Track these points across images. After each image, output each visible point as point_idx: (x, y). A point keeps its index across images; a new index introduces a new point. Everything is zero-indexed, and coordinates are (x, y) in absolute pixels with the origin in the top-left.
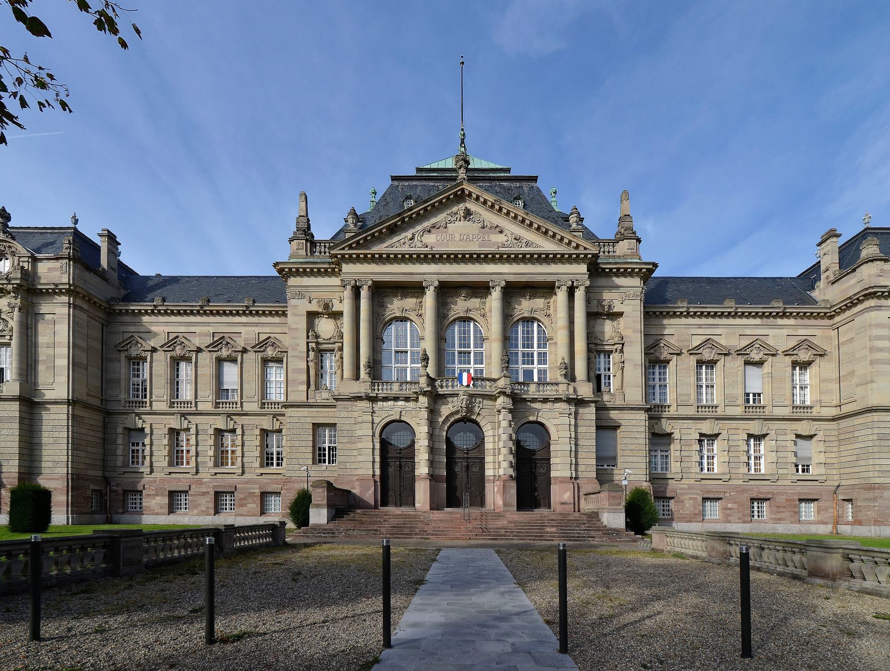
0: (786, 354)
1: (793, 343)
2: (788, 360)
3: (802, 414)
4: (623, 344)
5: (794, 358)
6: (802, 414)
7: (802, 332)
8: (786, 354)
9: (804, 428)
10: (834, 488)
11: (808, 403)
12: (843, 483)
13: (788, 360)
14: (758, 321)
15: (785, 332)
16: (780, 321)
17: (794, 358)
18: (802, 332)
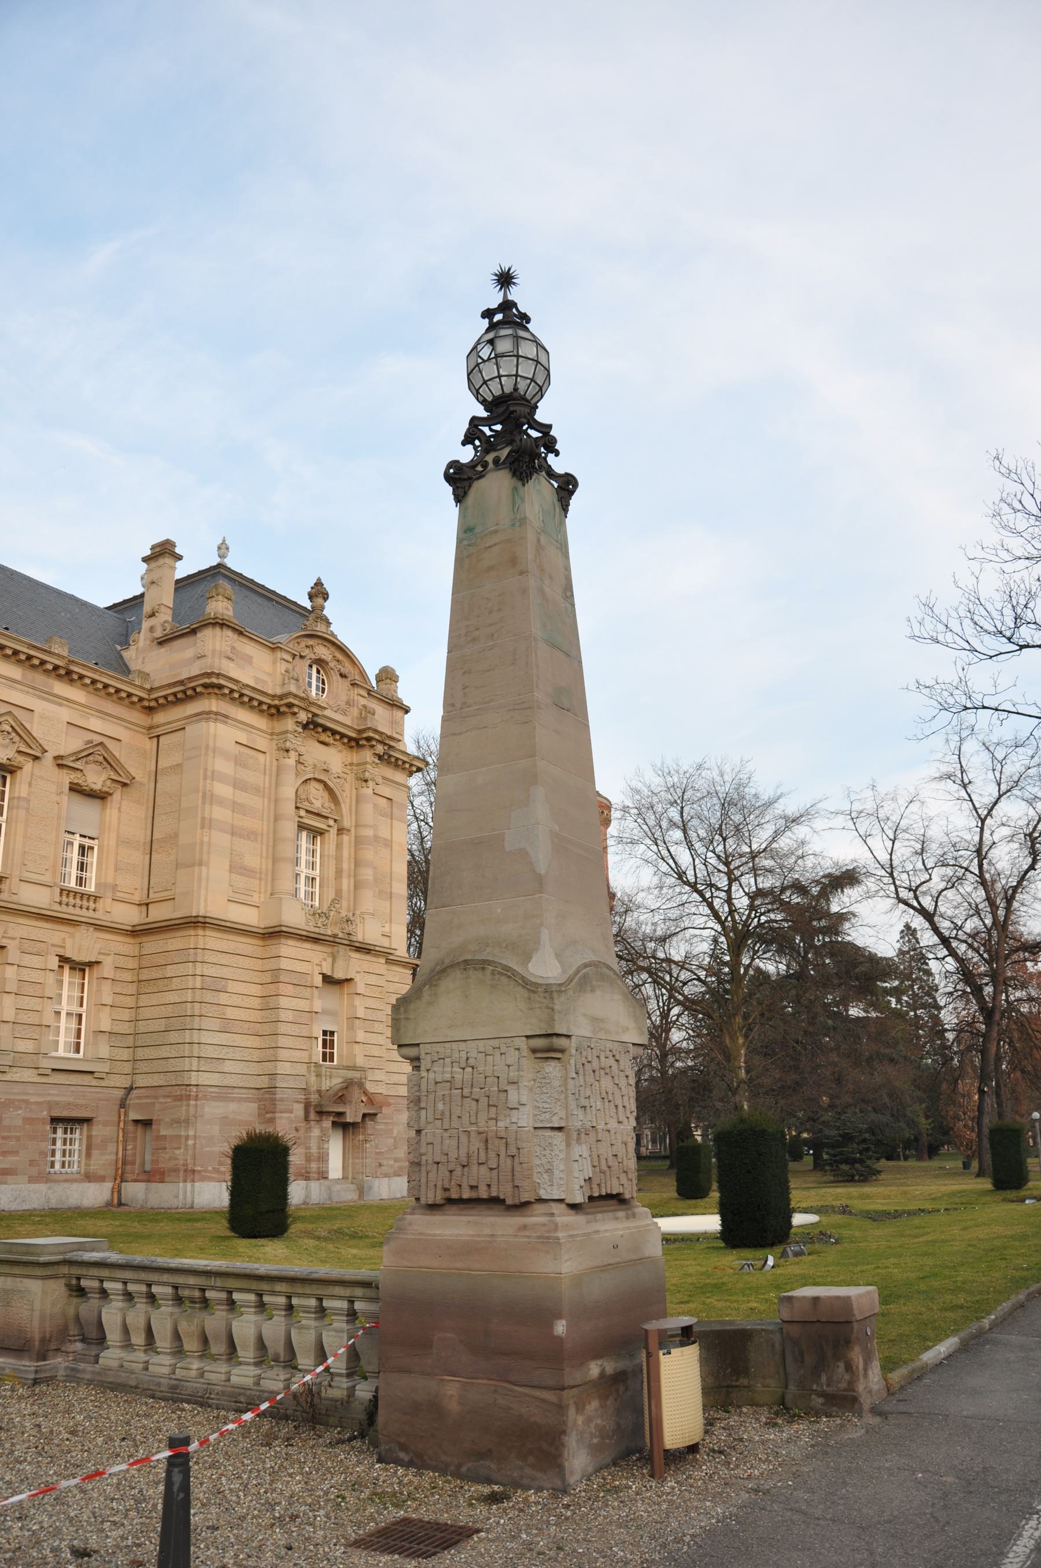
0: (60, 762)
1: (72, 744)
2: (67, 778)
3: (71, 910)
5: (74, 777)
6: (77, 911)
7: (96, 724)
8: (60, 762)
9: (82, 944)
10: (120, 1094)
11: (91, 888)
12: (141, 1081)
13: (67, 778)
15: (65, 714)
16: (61, 688)
17: (74, 777)
18: (96, 724)
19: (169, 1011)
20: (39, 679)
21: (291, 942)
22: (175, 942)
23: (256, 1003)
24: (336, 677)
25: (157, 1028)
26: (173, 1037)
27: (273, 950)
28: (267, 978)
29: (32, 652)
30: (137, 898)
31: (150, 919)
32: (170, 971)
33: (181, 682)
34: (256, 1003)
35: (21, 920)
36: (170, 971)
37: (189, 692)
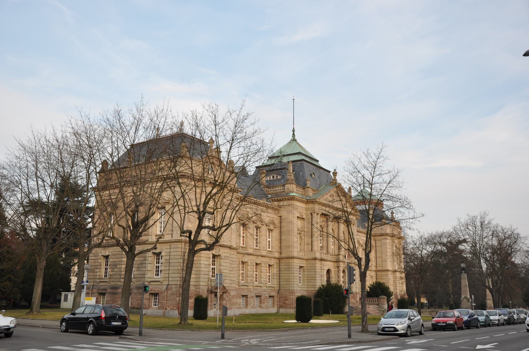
22: (384, 273)
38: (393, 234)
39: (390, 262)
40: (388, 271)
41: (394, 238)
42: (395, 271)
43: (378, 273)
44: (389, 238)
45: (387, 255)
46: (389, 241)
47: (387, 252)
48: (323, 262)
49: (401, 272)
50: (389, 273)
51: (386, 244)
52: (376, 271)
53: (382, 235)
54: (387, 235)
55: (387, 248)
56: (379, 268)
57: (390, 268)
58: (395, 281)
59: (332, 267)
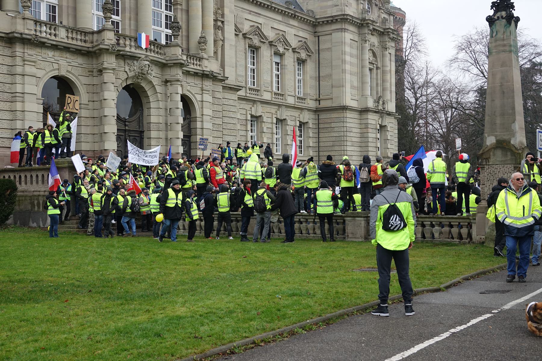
4: (223, 22)
14: (279, 18)
19: (334, 139)
20: (286, 19)
21: (370, 113)
22: (334, 115)
23: (358, 135)
24: (374, 6)
25: (329, 145)
26: (337, 148)
27: (365, 116)
28: (363, 126)
29: (286, 10)
30: (315, 98)
31: (320, 106)
32: (333, 125)
33: (332, 17)
34: (358, 135)
35: (289, 109)
36: (333, 125)
37: (334, 21)
38: (364, 20)
39: (352, 87)
40: (344, 108)
41: (366, 31)
42: (364, 111)
43: (323, 116)
44: (352, 28)
45: (344, 71)
46: (349, 36)
47: (344, 62)
48: (19, 49)
49: (382, 113)
50: (349, 114)
51: (343, 43)
52: (317, 111)
53: (332, 20)
54: (344, 19)
55: (343, 53)
56: (324, 104)
57: (350, 102)
58: (363, 136)
59: (78, 71)
